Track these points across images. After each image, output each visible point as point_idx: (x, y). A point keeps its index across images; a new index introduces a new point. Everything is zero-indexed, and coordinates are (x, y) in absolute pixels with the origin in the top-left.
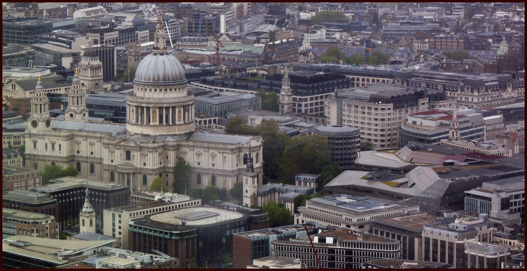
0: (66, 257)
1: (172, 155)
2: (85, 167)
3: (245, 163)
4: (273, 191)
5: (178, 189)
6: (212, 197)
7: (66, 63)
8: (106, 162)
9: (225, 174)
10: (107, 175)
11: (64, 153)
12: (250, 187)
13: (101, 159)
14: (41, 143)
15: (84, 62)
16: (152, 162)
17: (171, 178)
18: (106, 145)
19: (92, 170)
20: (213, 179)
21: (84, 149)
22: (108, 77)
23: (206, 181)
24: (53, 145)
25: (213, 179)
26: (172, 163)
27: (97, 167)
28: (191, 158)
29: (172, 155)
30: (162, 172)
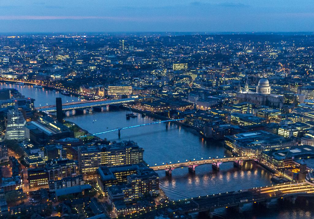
0: (244, 117)
1: (265, 98)
2: (248, 100)
3: (280, 100)
4: (286, 106)
5: (267, 106)
6: (274, 107)
7: (244, 80)
8: (252, 99)
9: (276, 103)
10: (252, 102)
11: (244, 97)
12: (281, 105)
13: (251, 99)
14: (239, 95)
15: (248, 80)
16: (261, 100)
17: (265, 103)
18: (252, 96)
19: (249, 101)
20: (274, 104)
21: (248, 97)
22: (252, 83)
23: (272, 104)
24: (242, 95)
25: (274, 104)
26: (265, 100)
27: (250, 100)
28: (269, 99)
29: (265, 98)
30: (263, 102)
